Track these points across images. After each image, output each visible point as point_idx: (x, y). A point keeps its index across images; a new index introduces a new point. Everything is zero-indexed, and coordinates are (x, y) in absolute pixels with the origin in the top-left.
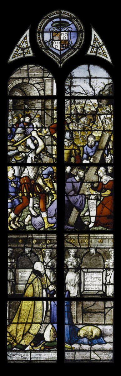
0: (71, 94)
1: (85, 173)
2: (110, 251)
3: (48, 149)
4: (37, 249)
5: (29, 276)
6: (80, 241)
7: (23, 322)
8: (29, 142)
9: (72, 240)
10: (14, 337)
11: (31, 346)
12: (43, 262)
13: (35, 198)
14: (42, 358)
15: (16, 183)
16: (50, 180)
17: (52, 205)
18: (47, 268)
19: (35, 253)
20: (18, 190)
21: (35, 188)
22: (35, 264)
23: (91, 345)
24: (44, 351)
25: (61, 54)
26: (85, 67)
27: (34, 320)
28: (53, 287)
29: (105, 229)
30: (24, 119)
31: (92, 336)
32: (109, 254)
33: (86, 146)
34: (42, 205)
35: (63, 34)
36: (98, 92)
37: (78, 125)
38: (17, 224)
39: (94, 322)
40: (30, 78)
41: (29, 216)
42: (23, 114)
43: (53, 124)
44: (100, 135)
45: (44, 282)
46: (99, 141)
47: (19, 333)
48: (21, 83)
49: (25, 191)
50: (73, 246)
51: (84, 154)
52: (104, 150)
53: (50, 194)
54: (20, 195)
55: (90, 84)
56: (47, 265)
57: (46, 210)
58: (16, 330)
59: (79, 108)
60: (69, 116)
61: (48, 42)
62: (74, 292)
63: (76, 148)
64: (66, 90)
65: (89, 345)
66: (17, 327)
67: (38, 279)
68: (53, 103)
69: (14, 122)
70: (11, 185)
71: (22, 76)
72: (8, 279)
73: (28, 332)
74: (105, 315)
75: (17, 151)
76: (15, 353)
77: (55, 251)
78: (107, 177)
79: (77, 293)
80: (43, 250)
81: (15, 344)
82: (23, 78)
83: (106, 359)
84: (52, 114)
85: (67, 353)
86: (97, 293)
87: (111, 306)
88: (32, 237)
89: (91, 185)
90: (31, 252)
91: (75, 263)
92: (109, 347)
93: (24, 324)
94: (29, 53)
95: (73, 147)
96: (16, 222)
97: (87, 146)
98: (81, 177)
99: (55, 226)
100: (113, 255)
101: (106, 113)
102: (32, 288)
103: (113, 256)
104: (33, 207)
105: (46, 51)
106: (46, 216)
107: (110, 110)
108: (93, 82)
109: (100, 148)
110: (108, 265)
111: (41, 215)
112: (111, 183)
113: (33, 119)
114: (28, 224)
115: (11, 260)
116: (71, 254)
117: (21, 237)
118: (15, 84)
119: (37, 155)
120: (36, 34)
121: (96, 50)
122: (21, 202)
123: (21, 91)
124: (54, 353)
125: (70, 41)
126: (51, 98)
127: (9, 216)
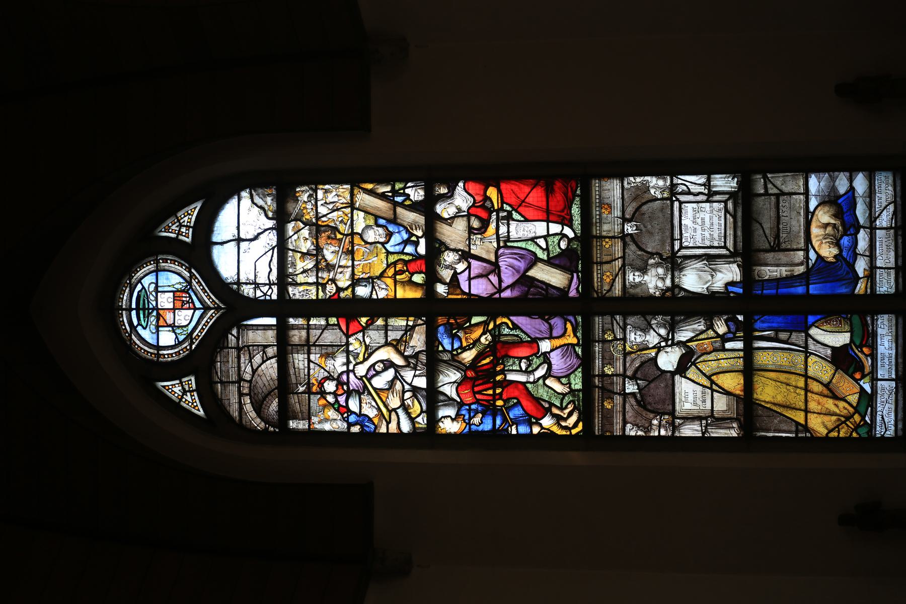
2: (629, 187)
4: (628, 365)
7: (803, 397)
8: (380, 382)
9: (604, 277)
10: (839, 420)
11: (860, 380)
12: (659, 348)
14: (890, 352)
15: (472, 414)
16: (466, 333)
20: (489, 409)
21: (485, 367)
23: (858, 227)
24: (874, 347)
26: (217, 251)
28: (718, 323)
29: (578, 199)
30: (330, 393)
31: (834, 226)
32: (637, 187)
33: (387, 246)
36: (268, 220)
37: (340, 266)
38: (567, 411)
39: (802, 220)
40: (240, 379)
41: (548, 382)
42: (319, 396)
44: (362, 214)
45: (707, 345)
46: (377, 217)
48: (250, 399)
49: (491, 392)
50: (620, 276)
51: (405, 251)
52: (396, 204)
53: (496, 335)
54: (499, 403)
55: (251, 240)
56: (666, 340)
57: (534, 342)
58: (822, 416)
60: (320, 288)
62: (730, 273)
64: (265, 294)
65: (858, 232)
66: (814, 413)
68: (294, 327)
69: (335, 417)
72: (701, 435)
73: (827, 386)
74: (783, 193)
75: (400, 411)
76: (879, 418)
77: (630, 320)
78: (456, 196)
79: (731, 265)
80: (630, 350)
81: (857, 418)
82: (241, 395)
83: (890, 188)
84: (316, 327)
86: (731, 215)
87: (762, 180)
88: (598, 376)
90: (634, 378)
91: (661, 271)
92: (860, 183)
93: (809, 394)
94: (190, 382)
96: (562, 414)
97: (385, 245)
98: (457, 257)
99: (571, 318)
100: (639, 179)
101: (312, 202)
102: (721, 375)
103: (642, 178)
104: (527, 372)
105: (194, 341)
106: (547, 340)
107: (308, 193)
109: (390, 215)
110: (664, 191)
111: (545, 353)
112: (472, 186)
113: (328, 372)
114: (566, 384)
115: (654, 427)
116: (638, 280)
117: (598, 403)
118: (253, 412)
119: (408, 366)
120: (161, 362)
121: (185, 228)
122: (515, 401)
124: (879, 322)
126: (282, 330)
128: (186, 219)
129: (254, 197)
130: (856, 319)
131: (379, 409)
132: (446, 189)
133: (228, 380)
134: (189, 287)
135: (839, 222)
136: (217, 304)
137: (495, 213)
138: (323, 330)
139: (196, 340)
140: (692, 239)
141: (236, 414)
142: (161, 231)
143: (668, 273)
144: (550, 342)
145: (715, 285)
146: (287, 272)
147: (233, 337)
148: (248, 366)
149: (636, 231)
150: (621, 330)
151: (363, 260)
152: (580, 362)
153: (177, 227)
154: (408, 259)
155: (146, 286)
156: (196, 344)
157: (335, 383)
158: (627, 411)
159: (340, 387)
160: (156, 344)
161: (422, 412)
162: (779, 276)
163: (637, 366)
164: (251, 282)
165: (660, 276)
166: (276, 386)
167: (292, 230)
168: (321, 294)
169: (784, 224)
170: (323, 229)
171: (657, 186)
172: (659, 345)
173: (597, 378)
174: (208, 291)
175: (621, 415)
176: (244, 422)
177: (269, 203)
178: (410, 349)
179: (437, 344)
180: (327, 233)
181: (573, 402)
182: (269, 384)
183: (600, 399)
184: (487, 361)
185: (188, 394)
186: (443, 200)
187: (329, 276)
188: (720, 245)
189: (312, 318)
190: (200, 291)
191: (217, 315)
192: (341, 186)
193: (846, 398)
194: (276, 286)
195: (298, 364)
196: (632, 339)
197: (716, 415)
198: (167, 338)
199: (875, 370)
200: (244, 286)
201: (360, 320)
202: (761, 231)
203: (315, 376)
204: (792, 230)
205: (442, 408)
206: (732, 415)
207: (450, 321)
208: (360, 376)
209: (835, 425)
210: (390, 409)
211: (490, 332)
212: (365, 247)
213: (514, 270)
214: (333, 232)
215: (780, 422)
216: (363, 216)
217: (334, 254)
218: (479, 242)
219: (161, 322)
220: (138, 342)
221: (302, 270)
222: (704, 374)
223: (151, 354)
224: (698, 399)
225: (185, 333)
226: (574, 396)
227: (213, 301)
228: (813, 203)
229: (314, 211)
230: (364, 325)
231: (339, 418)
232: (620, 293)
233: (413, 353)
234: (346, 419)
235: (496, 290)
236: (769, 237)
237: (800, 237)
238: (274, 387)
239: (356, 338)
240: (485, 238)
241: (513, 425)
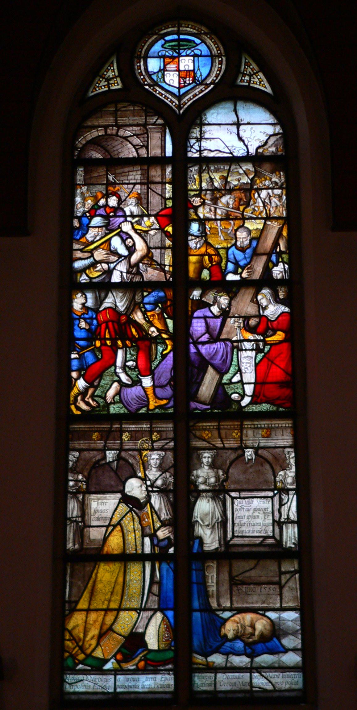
0: (201, 154)
1: (231, 299)
2: (286, 453)
3: (154, 254)
4: (131, 453)
5: (113, 509)
6: (223, 435)
7: (100, 607)
8: (116, 243)
9: (207, 432)
10: (80, 640)
11: (116, 659)
12: (144, 479)
13: (128, 349)
14: (140, 687)
15: (88, 321)
16: (158, 314)
17: (164, 362)
18: (153, 491)
19: (127, 461)
22: (127, 484)
23: (252, 656)
25: (181, 93)
26: (229, 106)
27: (124, 603)
29: (275, 408)
30: (107, 201)
33: (234, 248)
34: (142, 363)
35: (185, 60)
37: (215, 209)
39: (257, 605)
40: (119, 127)
41: (116, 385)
42: (104, 192)
43: (165, 208)
44: (260, 227)
46: (258, 239)
47: (91, 631)
48: (102, 135)
49: (107, 336)
50: (208, 445)
51: (229, 264)
52: (269, 255)
53: (158, 340)
56: (152, 486)
57: (151, 372)
58: (84, 624)
60: (198, 192)
61: (155, 73)
63: (213, 252)
64: (192, 147)
65: (248, 656)
66: (87, 617)
67: (133, 516)
69: (87, 206)
70: (78, 325)
73: (111, 629)
74: (281, 588)
75: (91, 260)
76: (80, 677)
77: (170, 455)
79: (217, 542)
80: (144, 454)
81: (81, 657)
82: (106, 127)
83: (287, 686)
84: (164, 190)
85: (197, 674)
86: (262, 541)
87: (293, 569)
88: (121, 427)
90: (119, 458)
91: (212, 480)
93: (103, 613)
95: (207, 249)
96: (88, 396)
97: (234, 247)
98: (224, 307)
99: (172, 403)
100: (292, 461)
102: (121, 534)
103: (294, 464)
104: (124, 367)
106: (152, 384)
107: (278, 181)
108: (245, 132)
110: (282, 483)
112: (286, 318)
113: (125, 200)
114: (114, 400)
115: (76, 476)
116: (205, 460)
117: (97, 428)
118: (91, 138)
119: (130, 266)
121: (248, 79)
122: (100, 357)
123: (101, 149)
125: (198, 72)
126: (162, 161)
127: (75, 385)
128: (256, 80)
129: (275, 137)
130: (170, 655)
131: (93, 242)
132: (282, 297)
133: (118, 117)
134: (198, 83)
135: (256, 639)
136: (183, 107)
137: (262, 338)
138: (161, 196)
139: (153, 90)
140: (240, 508)
142: (246, 59)
143: (210, 487)
144: (151, 386)
145: (200, 528)
147: (155, 120)
149: (247, 459)
150: (160, 447)
152: (133, 412)
153: (250, 72)
155: (199, 47)
156: (149, 89)
158: (91, 452)
159: (112, 210)
160: (149, 55)
161: (91, 278)
162: (208, 584)
163: (130, 460)
164: (202, 135)
165: (208, 480)
167: (247, 169)
168: (192, 193)
169: (254, 589)
170: (248, 194)
171: (287, 477)
172: (148, 479)
173: (119, 426)
174: (194, 99)
175: (87, 447)
177: (270, 149)
178: (145, 268)
180: (244, 198)
181: (99, 406)
182: (115, 151)
183: (101, 429)
185: (106, 83)
188: (235, 532)
189: (171, 186)
190: (195, 92)
191: (174, 107)
192: (285, 210)
193: (99, 646)
194: (198, 156)
195: (132, 175)
196: (153, 456)
197: (85, 530)
198: (154, 65)
199: (124, 672)
200: (198, 129)
202: (247, 568)
204: (249, 596)
205: (94, 295)
206: (85, 544)
207: (169, 302)
209: (75, 636)
210: (93, 252)
212: (232, 230)
213: (212, 354)
214: (245, 203)
215: (79, 587)
216: (259, 228)
217: (226, 204)
219: (168, 60)
220: (150, 40)
221: (213, 177)
222: (122, 519)
223: (141, 52)
224: (100, 514)
225: (159, 80)
226: (104, 407)
227: (186, 103)
228: (272, 615)
229: (264, 187)
230: (166, 229)
231: (86, 209)
232: (193, 445)
233: (142, 270)
235: (195, 339)
236: (242, 576)
237: (243, 604)
240: (241, 330)
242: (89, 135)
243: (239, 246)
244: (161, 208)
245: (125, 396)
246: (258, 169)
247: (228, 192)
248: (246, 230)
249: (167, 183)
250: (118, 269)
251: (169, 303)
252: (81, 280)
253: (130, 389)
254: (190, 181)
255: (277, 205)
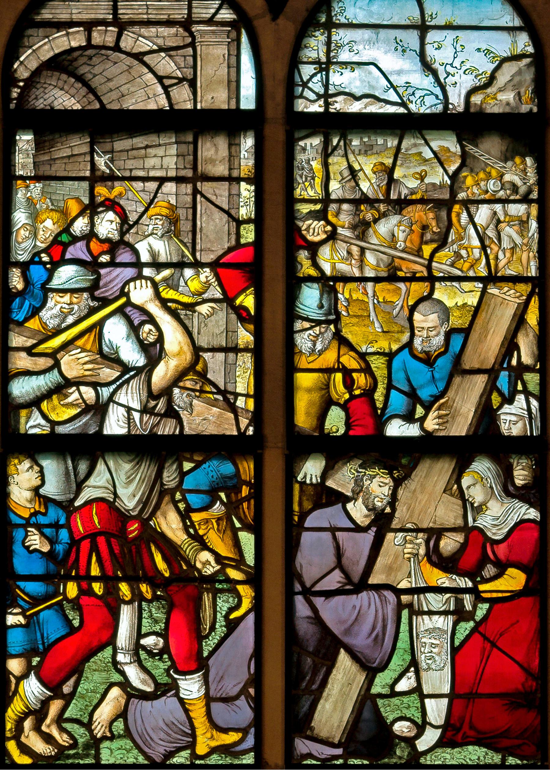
0: (327, 105)
1: (398, 483)
15: (47, 531)
16: (219, 520)
29: (497, 758)
30: (92, 224)
36: (464, 93)
37: (363, 250)
38: (55, 733)
41: (115, 692)
42: (86, 201)
43: (238, 245)
44: (473, 300)
46: (466, 332)
48: (80, 48)
49: (95, 571)
51: (393, 393)
55: (422, 55)
59: (368, 170)
60: (318, 207)
64: (305, 85)
68: (234, 145)
70: (23, 542)
71: (85, 16)
89: (427, 542)
95: (339, 357)
96: (48, 721)
97: (406, 350)
99: (250, 741)
106: (203, 691)
107: (519, 182)
108: (439, 48)
113: (137, 222)
118: (51, 54)
119: (151, 395)
122: (76, 623)
127: (16, 691)
129: (514, 62)
132: (522, 482)
137: (470, 584)
138: (227, 213)
141: (46, 14)
144: (199, 699)
146: (351, 133)
147: (213, 11)
148: (151, 44)
151: (376, 301)
154: (376, 398)
157: (115, 236)
159: (106, 246)
161: (53, 424)
164: (332, 54)
166: (108, 107)
168: (305, 209)
170: (444, 214)
176: (30, 32)
177: (502, 97)
178: (186, 399)
179: (196, 458)
180: (434, 223)
181: (74, 745)
182: (111, 90)
184: (161, 565)
186: (499, 476)
187: (343, 227)
192: (535, 256)
194: (321, 110)
195: (155, 156)
200: (322, 38)
201: (247, 292)
203: (130, 193)
207: (244, 487)
208: (129, 291)
210: (58, 356)
211: (223, 571)
212: (402, 307)
213: (350, 622)
214: (436, 237)
216: (470, 303)
218: (410, 550)
221: (357, 167)
226: (87, 746)
229: (482, 197)
230: (238, 302)
231: (38, 243)
233: (179, 406)
234: (37, 259)
235: (308, 585)
238: (105, 102)
239: (210, 285)
241: (25, 617)
242: (46, 47)
243: (420, 349)
244: (226, 246)
245: (139, 722)
246: (470, 148)
247: (394, 208)
248: (437, 308)
249: (244, 180)
250: (121, 401)
251: (245, 491)
252: (28, 426)
253: (150, 702)
254: (301, 177)
255: (516, 244)
